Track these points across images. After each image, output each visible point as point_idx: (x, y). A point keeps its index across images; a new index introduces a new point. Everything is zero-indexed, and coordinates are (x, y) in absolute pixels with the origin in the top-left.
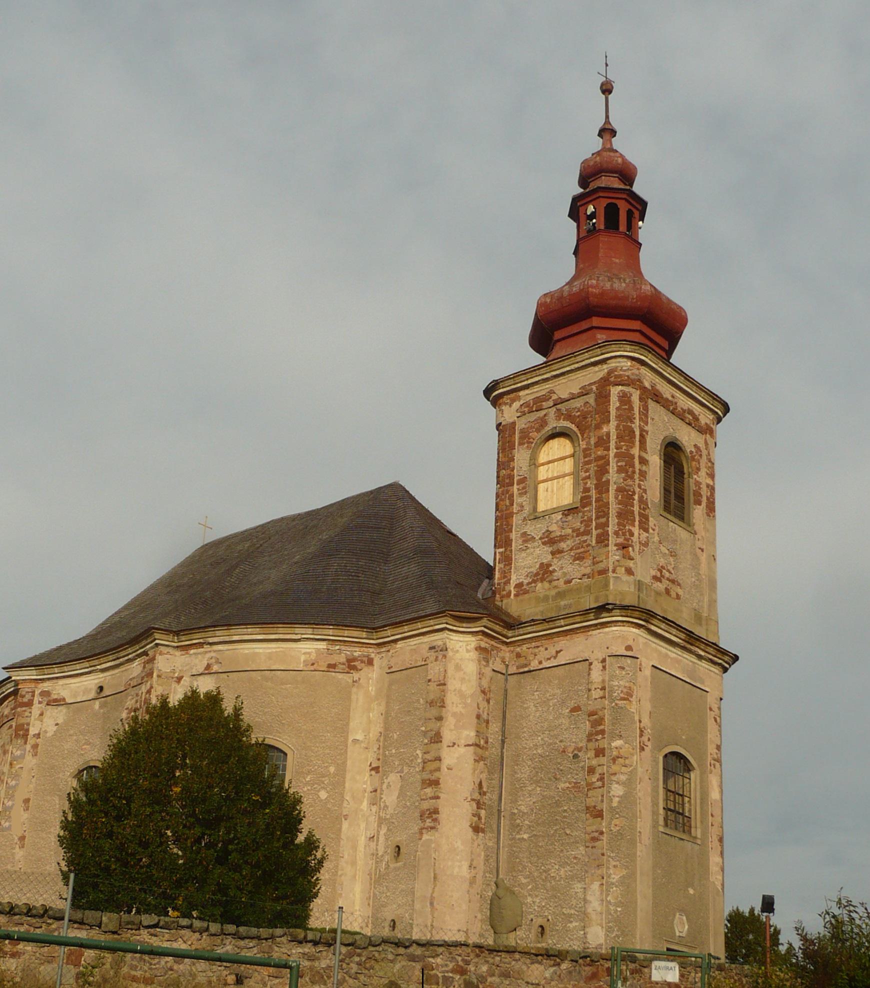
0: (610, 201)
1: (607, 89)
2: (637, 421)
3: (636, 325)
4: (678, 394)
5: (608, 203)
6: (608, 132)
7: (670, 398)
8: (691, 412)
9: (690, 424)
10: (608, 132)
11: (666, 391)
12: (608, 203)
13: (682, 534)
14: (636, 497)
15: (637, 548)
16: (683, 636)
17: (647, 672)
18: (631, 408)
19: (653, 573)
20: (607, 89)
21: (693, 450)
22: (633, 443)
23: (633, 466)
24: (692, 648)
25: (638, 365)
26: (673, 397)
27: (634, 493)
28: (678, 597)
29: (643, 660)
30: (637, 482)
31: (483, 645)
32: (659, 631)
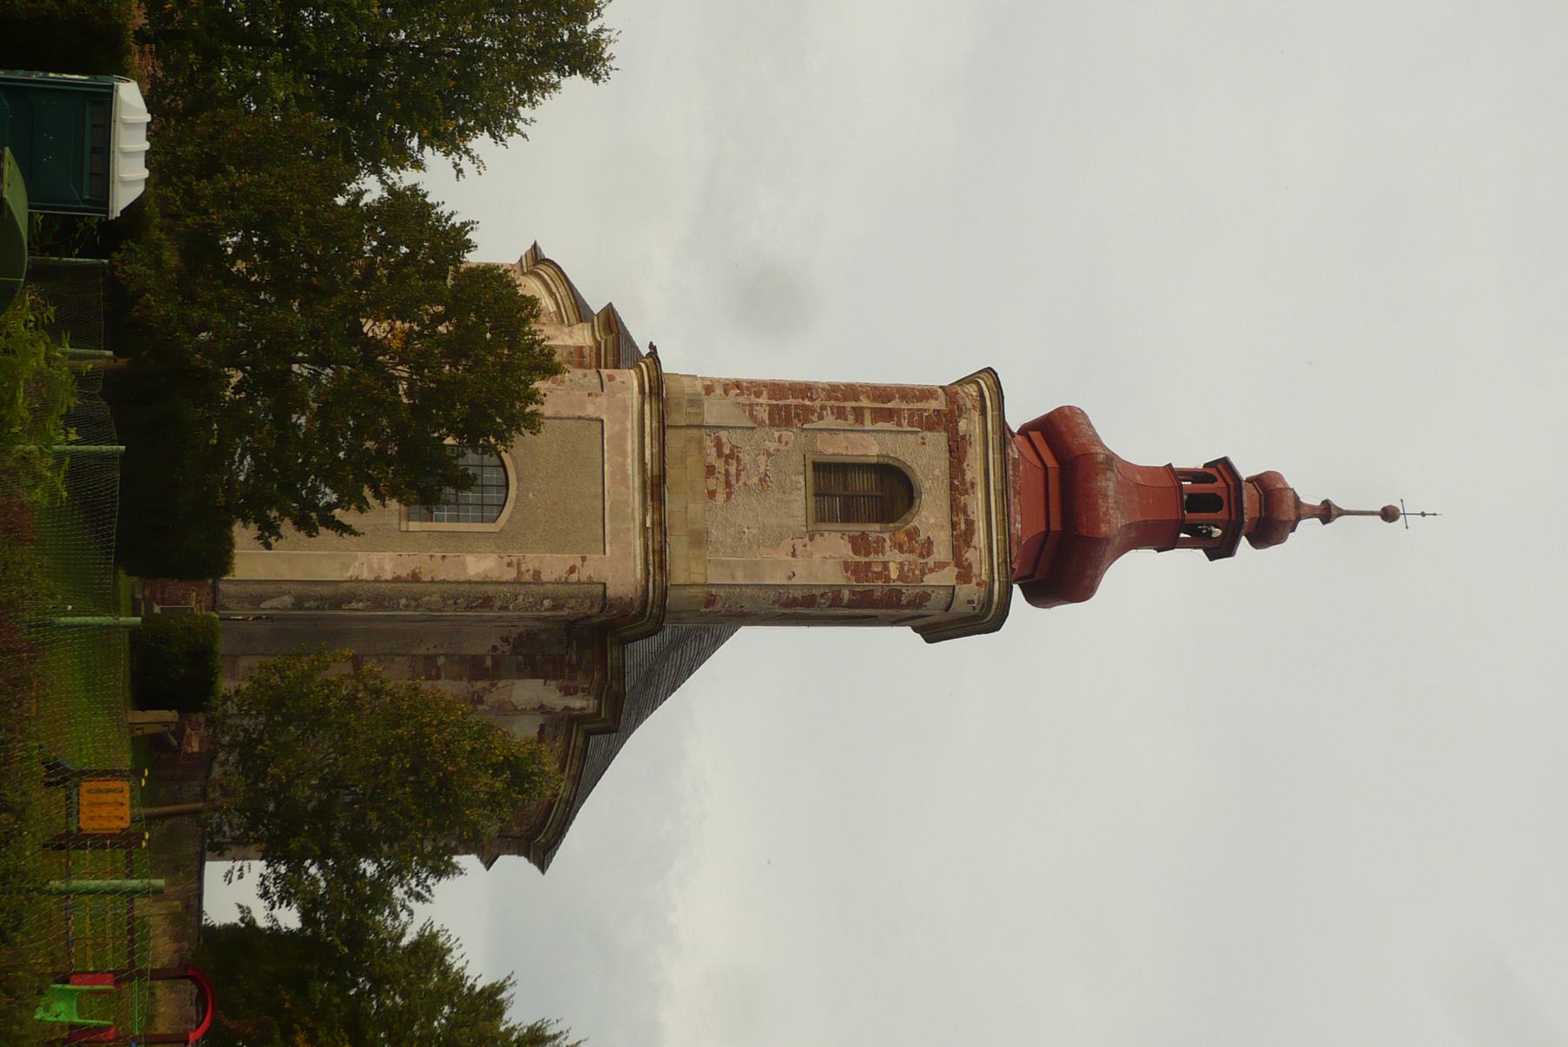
0: (1225, 499)
1: (1389, 514)
2: (904, 406)
3: (1051, 462)
4: (980, 494)
5: (1224, 510)
6: (1327, 513)
7: (968, 477)
8: (970, 524)
9: (954, 525)
10: (1327, 513)
11: (973, 471)
12: (1224, 510)
13: (797, 502)
14: (807, 402)
15: (740, 399)
16: (656, 472)
17: (590, 410)
18: (920, 400)
19: (724, 435)
20: (1389, 514)
21: (923, 536)
22: (874, 400)
23: (845, 400)
24: (649, 502)
25: (977, 405)
26: (973, 485)
27: (811, 399)
28: (712, 494)
29: (603, 400)
30: (829, 403)
31: (586, 352)
32: (647, 422)
